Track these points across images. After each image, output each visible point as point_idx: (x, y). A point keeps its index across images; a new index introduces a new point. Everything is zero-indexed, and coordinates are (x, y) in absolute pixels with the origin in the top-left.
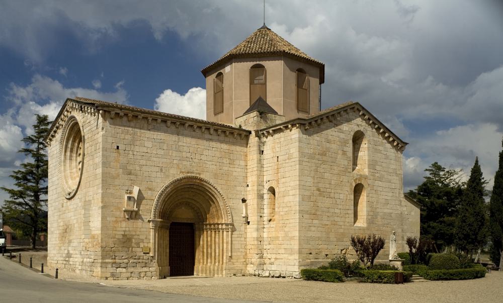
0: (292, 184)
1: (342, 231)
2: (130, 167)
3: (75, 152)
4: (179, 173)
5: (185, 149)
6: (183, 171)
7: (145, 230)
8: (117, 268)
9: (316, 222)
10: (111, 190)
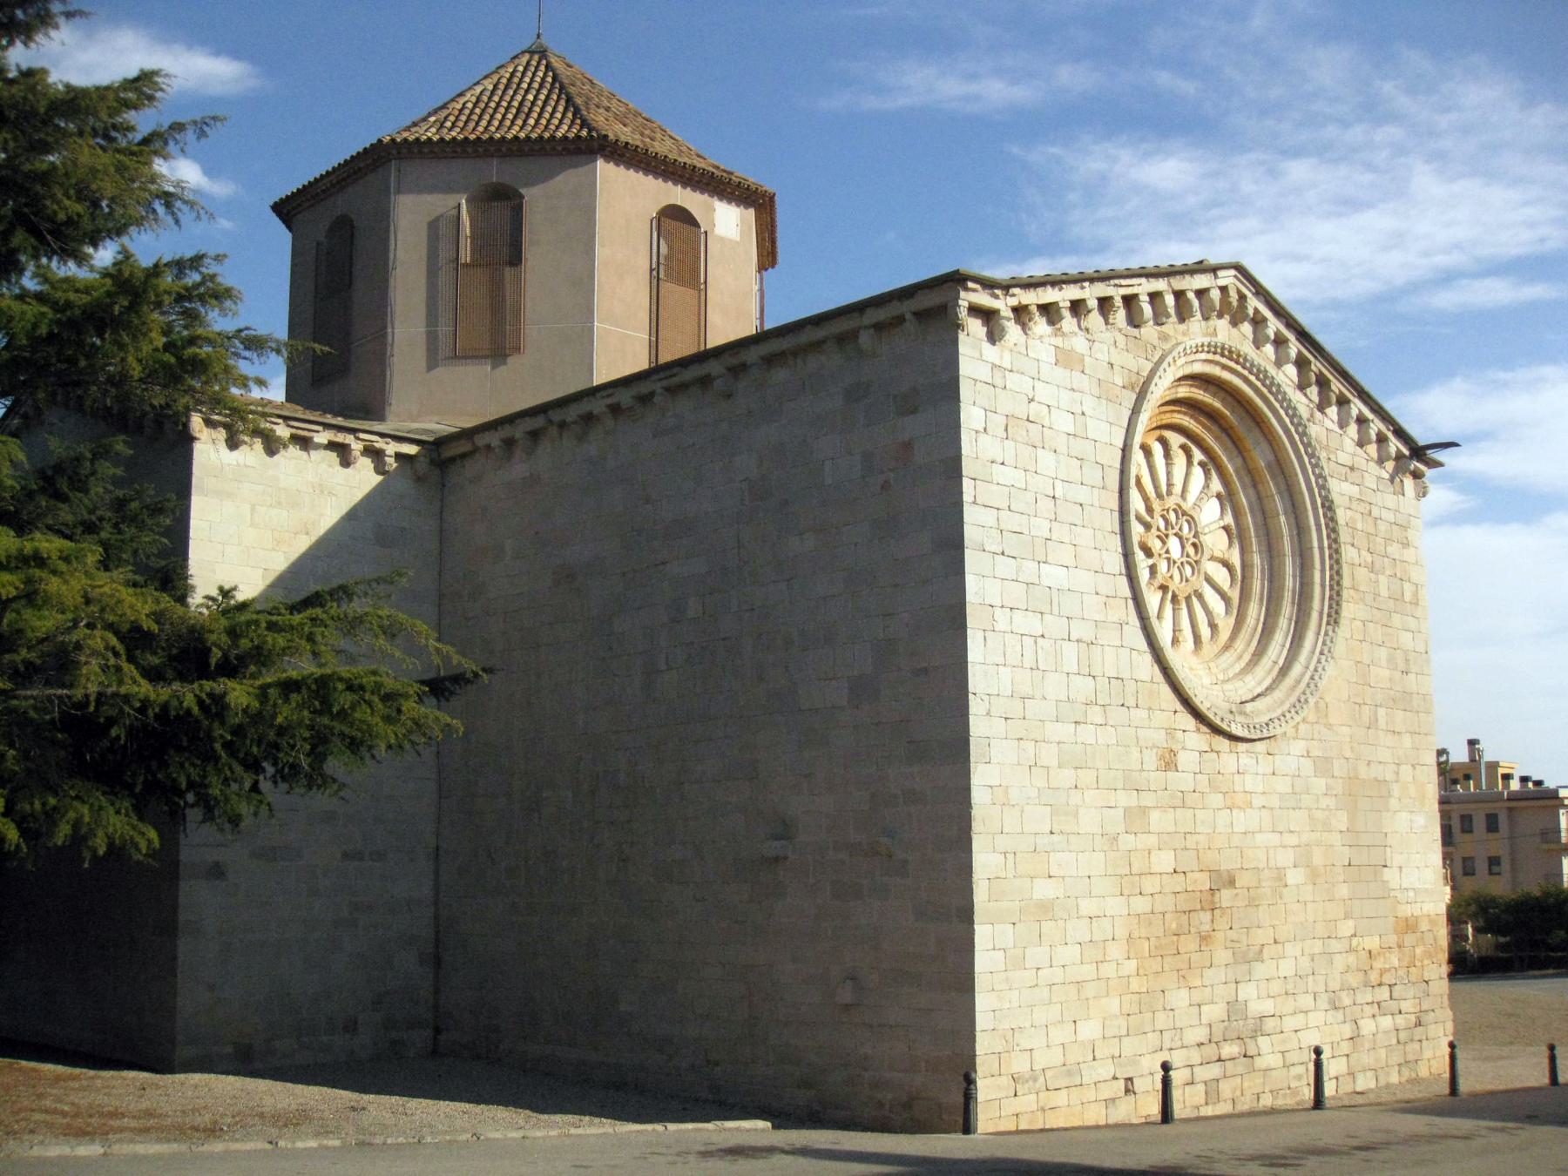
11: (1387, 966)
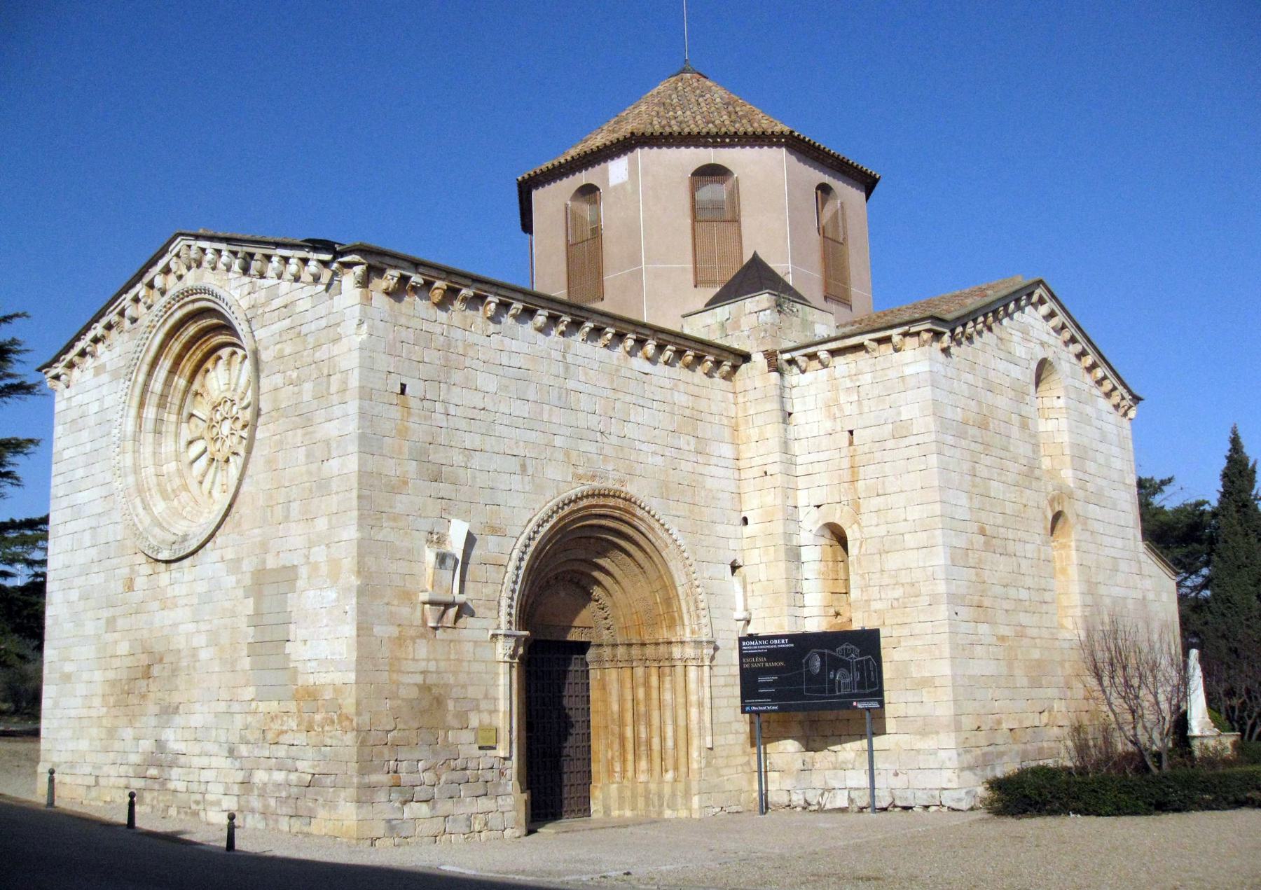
0: (915, 513)
1: (1036, 654)
2: (437, 456)
3: (175, 408)
4: (570, 479)
5: (584, 403)
6: (580, 471)
7: (482, 667)
8: (405, 803)
9: (983, 628)
10: (385, 531)
11: (285, 728)
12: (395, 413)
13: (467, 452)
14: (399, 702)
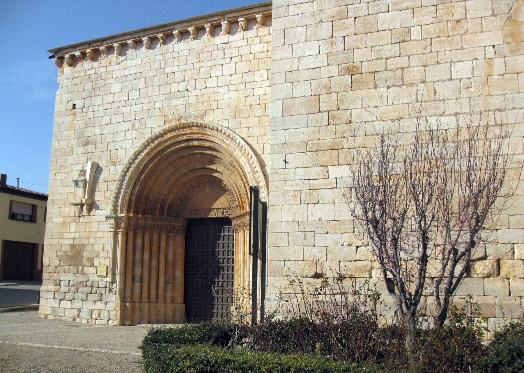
2: (88, 132)
12: (69, 119)
13: (102, 127)
14: (62, 252)
